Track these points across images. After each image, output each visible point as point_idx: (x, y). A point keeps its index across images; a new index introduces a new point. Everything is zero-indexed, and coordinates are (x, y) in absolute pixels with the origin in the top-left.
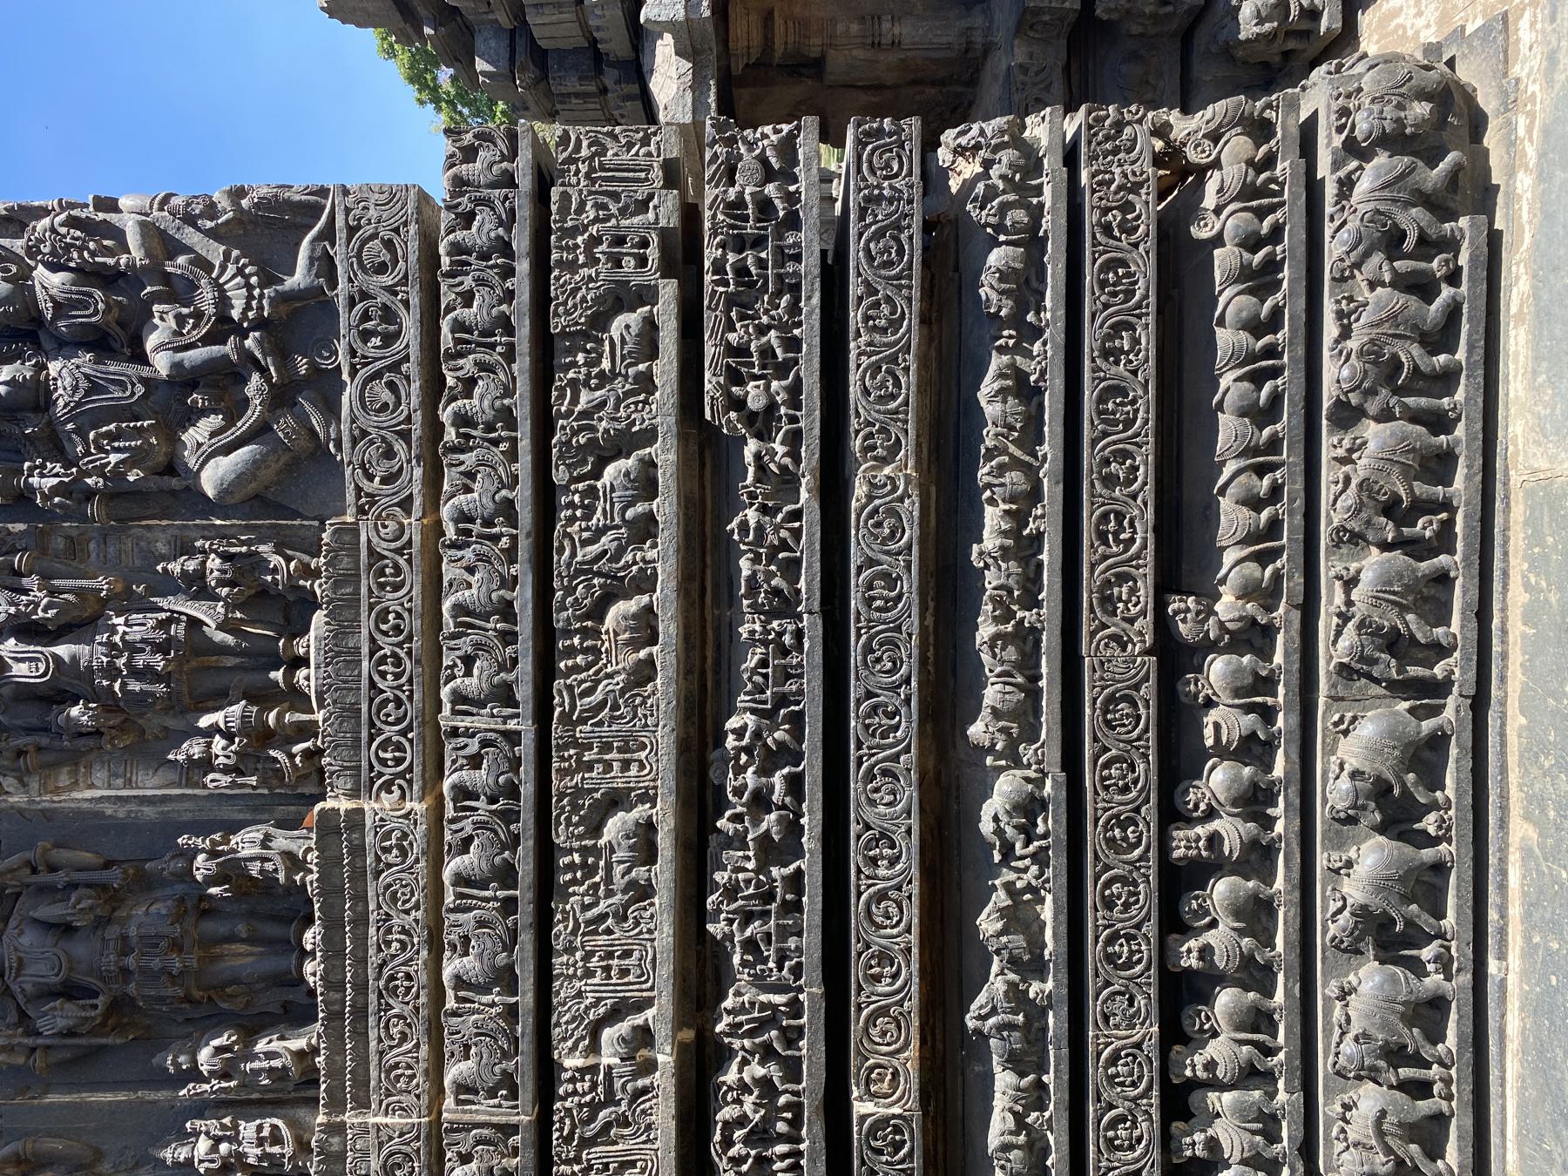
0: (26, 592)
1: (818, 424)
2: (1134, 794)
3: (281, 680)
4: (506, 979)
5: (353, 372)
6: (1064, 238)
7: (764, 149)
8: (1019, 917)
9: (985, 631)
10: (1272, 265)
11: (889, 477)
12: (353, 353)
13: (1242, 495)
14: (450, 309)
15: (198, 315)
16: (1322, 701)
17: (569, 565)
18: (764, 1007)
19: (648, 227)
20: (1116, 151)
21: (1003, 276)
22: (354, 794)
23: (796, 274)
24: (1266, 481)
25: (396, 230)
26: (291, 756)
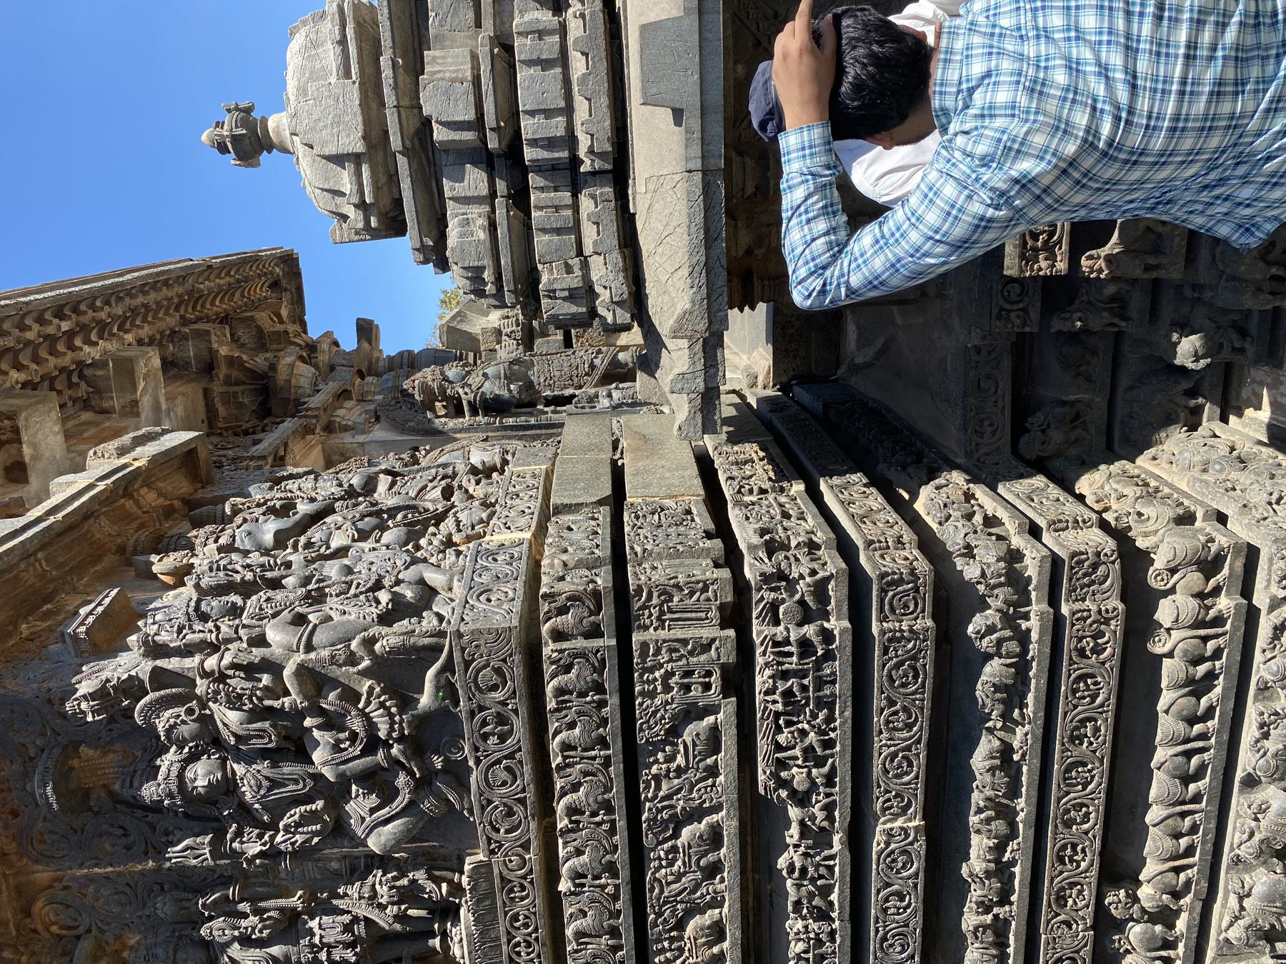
0: (245, 916)
1: (849, 799)
3: (438, 949)
5: (478, 762)
6: (1048, 661)
7: (803, 595)
9: (970, 920)
10: (1211, 676)
11: (902, 828)
12: (477, 750)
13: (1169, 832)
14: (556, 733)
15: (353, 737)
17: (658, 899)
19: (712, 662)
20: (1092, 583)
23: (833, 695)
24: (1188, 821)
25: (504, 660)
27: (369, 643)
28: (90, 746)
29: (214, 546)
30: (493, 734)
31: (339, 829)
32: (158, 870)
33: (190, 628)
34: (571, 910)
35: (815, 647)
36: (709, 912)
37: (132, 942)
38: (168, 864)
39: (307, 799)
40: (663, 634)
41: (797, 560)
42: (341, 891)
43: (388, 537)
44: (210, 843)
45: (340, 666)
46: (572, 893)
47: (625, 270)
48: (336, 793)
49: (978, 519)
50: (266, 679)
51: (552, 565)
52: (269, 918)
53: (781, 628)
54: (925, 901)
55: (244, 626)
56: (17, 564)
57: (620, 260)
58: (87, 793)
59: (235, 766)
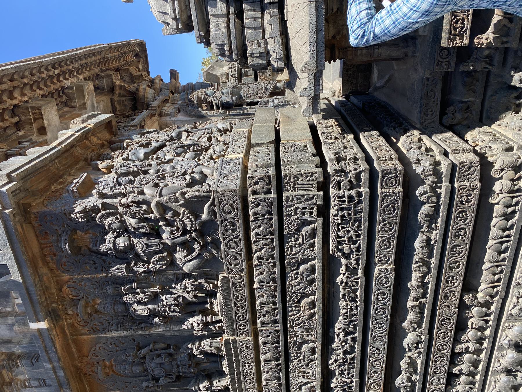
0: (139, 294)
1: (365, 257)
2: (446, 339)
4: (279, 379)
5: (224, 240)
6: (447, 206)
8: (412, 364)
9: (410, 303)
10: (514, 212)
11: (386, 269)
12: (224, 235)
14: (254, 229)
15: (178, 229)
16: (504, 319)
17: (291, 292)
18: (344, 382)
19: (314, 204)
20: (468, 174)
21: (426, 216)
22: (233, 335)
23: (361, 217)
24: (499, 269)
25: (234, 202)
26: (215, 328)
27: (183, 194)
28: (80, 231)
29: (121, 158)
30: (230, 229)
31: (172, 263)
32: (107, 277)
33: (115, 188)
34: (258, 295)
35: (354, 199)
36: (310, 297)
37: (98, 302)
38: (110, 275)
39: (161, 252)
40: (295, 193)
41: (349, 164)
42: (173, 286)
43: (187, 156)
44: (126, 267)
45: (172, 203)
46: (259, 288)
47: (282, 45)
48: (171, 250)
49: (423, 149)
50: (144, 207)
51: (252, 166)
52: (147, 295)
53: (341, 191)
54: (393, 296)
55: (135, 187)
56: (48, 164)
57: (280, 40)
58: (80, 248)
59: (134, 239)
